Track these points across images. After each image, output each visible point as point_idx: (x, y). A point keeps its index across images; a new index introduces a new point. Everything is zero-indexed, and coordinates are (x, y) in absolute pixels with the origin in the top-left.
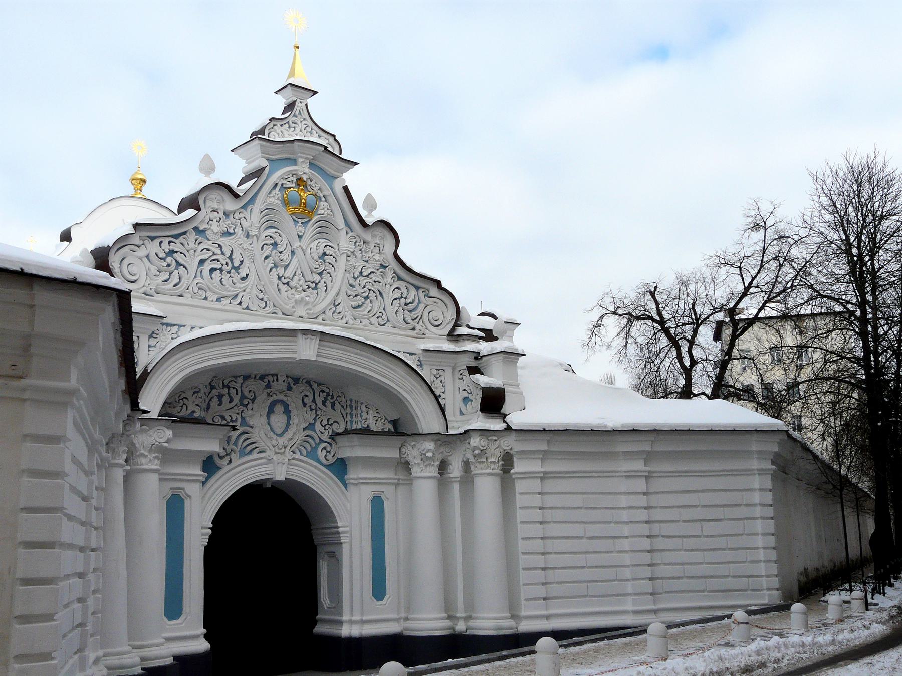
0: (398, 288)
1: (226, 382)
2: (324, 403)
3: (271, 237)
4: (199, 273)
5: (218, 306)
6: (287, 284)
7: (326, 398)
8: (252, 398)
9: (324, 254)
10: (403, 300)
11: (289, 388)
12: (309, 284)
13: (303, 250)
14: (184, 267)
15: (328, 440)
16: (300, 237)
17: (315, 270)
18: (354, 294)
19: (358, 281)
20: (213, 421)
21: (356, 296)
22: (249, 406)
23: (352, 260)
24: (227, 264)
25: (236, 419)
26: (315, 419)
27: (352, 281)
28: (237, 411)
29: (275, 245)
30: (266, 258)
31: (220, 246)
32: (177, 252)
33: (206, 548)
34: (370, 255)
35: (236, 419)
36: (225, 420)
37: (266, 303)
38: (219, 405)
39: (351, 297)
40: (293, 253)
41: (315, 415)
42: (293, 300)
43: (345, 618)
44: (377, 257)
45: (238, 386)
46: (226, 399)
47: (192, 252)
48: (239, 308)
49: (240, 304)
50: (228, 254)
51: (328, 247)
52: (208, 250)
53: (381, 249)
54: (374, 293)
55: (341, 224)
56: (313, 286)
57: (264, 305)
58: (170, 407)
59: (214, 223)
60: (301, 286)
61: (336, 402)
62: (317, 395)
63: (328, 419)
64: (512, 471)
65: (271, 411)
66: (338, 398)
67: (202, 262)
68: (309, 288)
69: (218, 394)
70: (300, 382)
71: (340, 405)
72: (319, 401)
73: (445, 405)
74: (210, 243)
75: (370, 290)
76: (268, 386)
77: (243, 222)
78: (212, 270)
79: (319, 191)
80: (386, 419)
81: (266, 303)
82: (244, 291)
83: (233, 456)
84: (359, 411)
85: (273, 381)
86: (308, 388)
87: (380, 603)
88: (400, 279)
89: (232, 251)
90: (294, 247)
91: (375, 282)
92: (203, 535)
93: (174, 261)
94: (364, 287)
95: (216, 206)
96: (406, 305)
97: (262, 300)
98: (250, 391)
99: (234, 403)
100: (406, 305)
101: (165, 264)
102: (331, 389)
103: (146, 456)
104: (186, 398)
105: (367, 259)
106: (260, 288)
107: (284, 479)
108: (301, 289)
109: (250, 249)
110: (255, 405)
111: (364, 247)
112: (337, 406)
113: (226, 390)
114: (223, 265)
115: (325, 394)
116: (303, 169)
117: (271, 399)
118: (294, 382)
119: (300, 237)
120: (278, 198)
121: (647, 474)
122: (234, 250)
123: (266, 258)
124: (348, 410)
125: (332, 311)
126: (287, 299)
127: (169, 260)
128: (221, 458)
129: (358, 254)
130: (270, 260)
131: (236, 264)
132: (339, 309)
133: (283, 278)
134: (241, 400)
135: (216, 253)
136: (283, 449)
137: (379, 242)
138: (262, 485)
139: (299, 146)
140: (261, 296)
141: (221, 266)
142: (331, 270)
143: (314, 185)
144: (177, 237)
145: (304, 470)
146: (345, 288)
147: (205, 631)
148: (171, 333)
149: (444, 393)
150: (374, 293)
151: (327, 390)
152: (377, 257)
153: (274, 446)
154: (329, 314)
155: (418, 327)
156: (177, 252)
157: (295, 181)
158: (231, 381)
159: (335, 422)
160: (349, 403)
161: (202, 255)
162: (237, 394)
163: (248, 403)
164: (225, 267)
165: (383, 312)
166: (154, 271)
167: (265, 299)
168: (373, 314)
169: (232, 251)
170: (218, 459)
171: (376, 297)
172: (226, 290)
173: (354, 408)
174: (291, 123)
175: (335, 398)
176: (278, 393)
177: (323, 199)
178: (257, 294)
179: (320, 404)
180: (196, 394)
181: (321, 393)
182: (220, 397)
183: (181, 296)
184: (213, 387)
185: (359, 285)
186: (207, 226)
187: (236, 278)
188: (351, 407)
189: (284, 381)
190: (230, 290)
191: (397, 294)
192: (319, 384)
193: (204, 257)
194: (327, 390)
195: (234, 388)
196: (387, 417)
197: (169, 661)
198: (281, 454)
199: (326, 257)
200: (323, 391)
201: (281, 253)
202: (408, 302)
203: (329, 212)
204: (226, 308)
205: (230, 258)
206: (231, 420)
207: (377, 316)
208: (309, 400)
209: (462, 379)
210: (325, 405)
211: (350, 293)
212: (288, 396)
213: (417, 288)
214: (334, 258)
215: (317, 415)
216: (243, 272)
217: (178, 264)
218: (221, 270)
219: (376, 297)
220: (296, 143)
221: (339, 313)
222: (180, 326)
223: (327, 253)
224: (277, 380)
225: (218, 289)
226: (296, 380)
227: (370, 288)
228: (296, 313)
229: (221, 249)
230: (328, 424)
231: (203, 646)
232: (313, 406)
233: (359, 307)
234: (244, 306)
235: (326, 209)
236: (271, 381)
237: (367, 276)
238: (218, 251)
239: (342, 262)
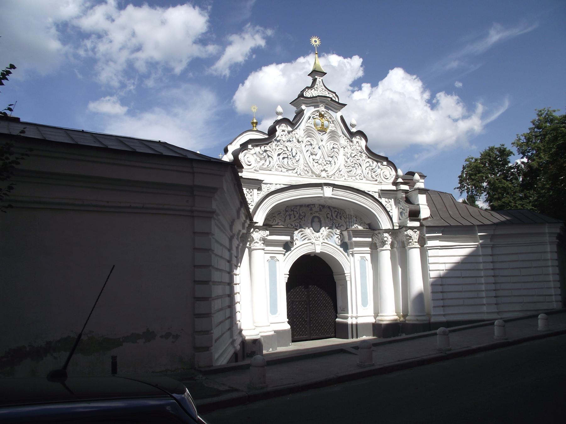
0: (368, 162)
1: (292, 209)
2: (336, 217)
3: (309, 141)
4: (278, 160)
5: (287, 174)
6: (317, 162)
9: (333, 148)
10: (371, 168)
11: (320, 210)
12: (327, 162)
13: (324, 147)
14: (271, 157)
15: (339, 234)
16: (322, 141)
17: (329, 155)
18: (348, 166)
19: (349, 159)
20: (288, 226)
21: (349, 166)
22: (303, 219)
25: (297, 225)
26: (332, 224)
27: (346, 159)
28: (298, 222)
29: (311, 145)
30: (307, 151)
31: (287, 147)
32: (268, 151)
33: (287, 283)
34: (354, 147)
35: (297, 225)
36: (292, 226)
37: (308, 172)
38: (290, 219)
39: (346, 167)
40: (319, 148)
41: (332, 222)
42: (320, 170)
43: (350, 314)
44: (358, 148)
45: (297, 210)
46: (292, 216)
47: (274, 150)
48: (296, 175)
49: (297, 173)
50: (290, 150)
52: (281, 149)
53: (360, 144)
54: (357, 164)
55: (341, 134)
56: (329, 163)
57: (307, 173)
58: (268, 221)
59: (283, 137)
60: (323, 163)
61: (342, 216)
62: (333, 213)
63: (339, 224)
64: (425, 246)
65: (312, 221)
66: (343, 214)
67: (279, 155)
68: (327, 164)
69: (289, 214)
70: (325, 207)
72: (334, 215)
73: (392, 215)
74: (282, 146)
75: (355, 163)
76: (311, 209)
77: (296, 135)
78: (284, 158)
80: (365, 223)
81: (308, 172)
82: (298, 167)
83: (296, 242)
84: (352, 219)
85: (313, 207)
86: (329, 210)
87: (365, 308)
88: (369, 158)
89: (292, 149)
90: (320, 145)
91: (357, 159)
92: (285, 277)
93: (267, 155)
94: (352, 162)
95: (284, 128)
96: (372, 169)
97: (306, 170)
98: (303, 212)
99: (296, 218)
100: (372, 169)
101: (263, 157)
103: (258, 243)
104: (275, 217)
105: (353, 149)
106: (305, 165)
107: (320, 252)
108: (323, 165)
109: (300, 147)
111: (351, 144)
112: (343, 218)
113: (292, 212)
114: (288, 156)
115: (337, 212)
116: (322, 109)
119: (322, 141)
121: (492, 246)
122: (293, 148)
123: (307, 151)
124: (348, 220)
125: (338, 174)
126: (317, 169)
127: (265, 154)
129: (349, 147)
130: (309, 152)
132: (341, 173)
133: (315, 160)
134: (299, 217)
135: (285, 150)
136: (319, 239)
137: (358, 141)
138: (310, 255)
139: (319, 99)
140: (305, 169)
141: (287, 156)
142: (337, 155)
143: (327, 116)
144: (267, 144)
145: (329, 248)
146: (344, 163)
147: (288, 320)
148: (267, 187)
149: (392, 210)
150: (357, 164)
151: (338, 211)
152: (358, 148)
153: (315, 237)
154: (336, 175)
155: (378, 180)
156: (268, 151)
157: (318, 115)
159: (341, 225)
160: (347, 216)
161: (279, 151)
162: (297, 213)
163: (302, 218)
164: (289, 156)
166: (258, 159)
167: (308, 170)
168: (357, 175)
169: (292, 149)
170: (290, 243)
171: (358, 166)
172: (290, 167)
173: (350, 219)
174: (315, 88)
175: (341, 214)
176: (315, 213)
177: (332, 122)
178: (304, 168)
179: (334, 217)
180: (279, 215)
182: (290, 215)
183: (270, 170)
184: (286, 211)
185: (350, 161)
186: (281, 138)
187: (294, 161)
188: (349, 218)
189: (318, 207)
190: (292, 167)
191: (368, 164)
192: (334, 208)
193: (280, 152)
194: (338, 211)
196: (366, 222)
197: (273, 333)
198: (318, 240)
200: (335, 211)
201: (314, 148)
202: (373, 168)
203: (335, 128)
204: (290, 175)
206: (295, 226)
207: (359, 175)
209: (399, 203)
210: (337, 218)
211: (346, 165)
212: (320, 214)
213: (377, 162)
214: (338, 149)
216: (297, 158)
217: (269, 156)
218: (287, 157)
219: (358, 166)
220: (318, 98)
222: (270, 184)
223: (335, 147)
224: (315, 207)
225: (286, 166)
226: (323, 206)
227: (355, 162)
228: (321, 176)
229: (287, 148)
230: (338, 226)
231: (288, 327)
232: (331, 219)
233: (350, 171)
234: (298, 173)
235: (333, 127)
236: (312, 206)
237: (354, 157)
238: (285, 149)
239: (342, 151)
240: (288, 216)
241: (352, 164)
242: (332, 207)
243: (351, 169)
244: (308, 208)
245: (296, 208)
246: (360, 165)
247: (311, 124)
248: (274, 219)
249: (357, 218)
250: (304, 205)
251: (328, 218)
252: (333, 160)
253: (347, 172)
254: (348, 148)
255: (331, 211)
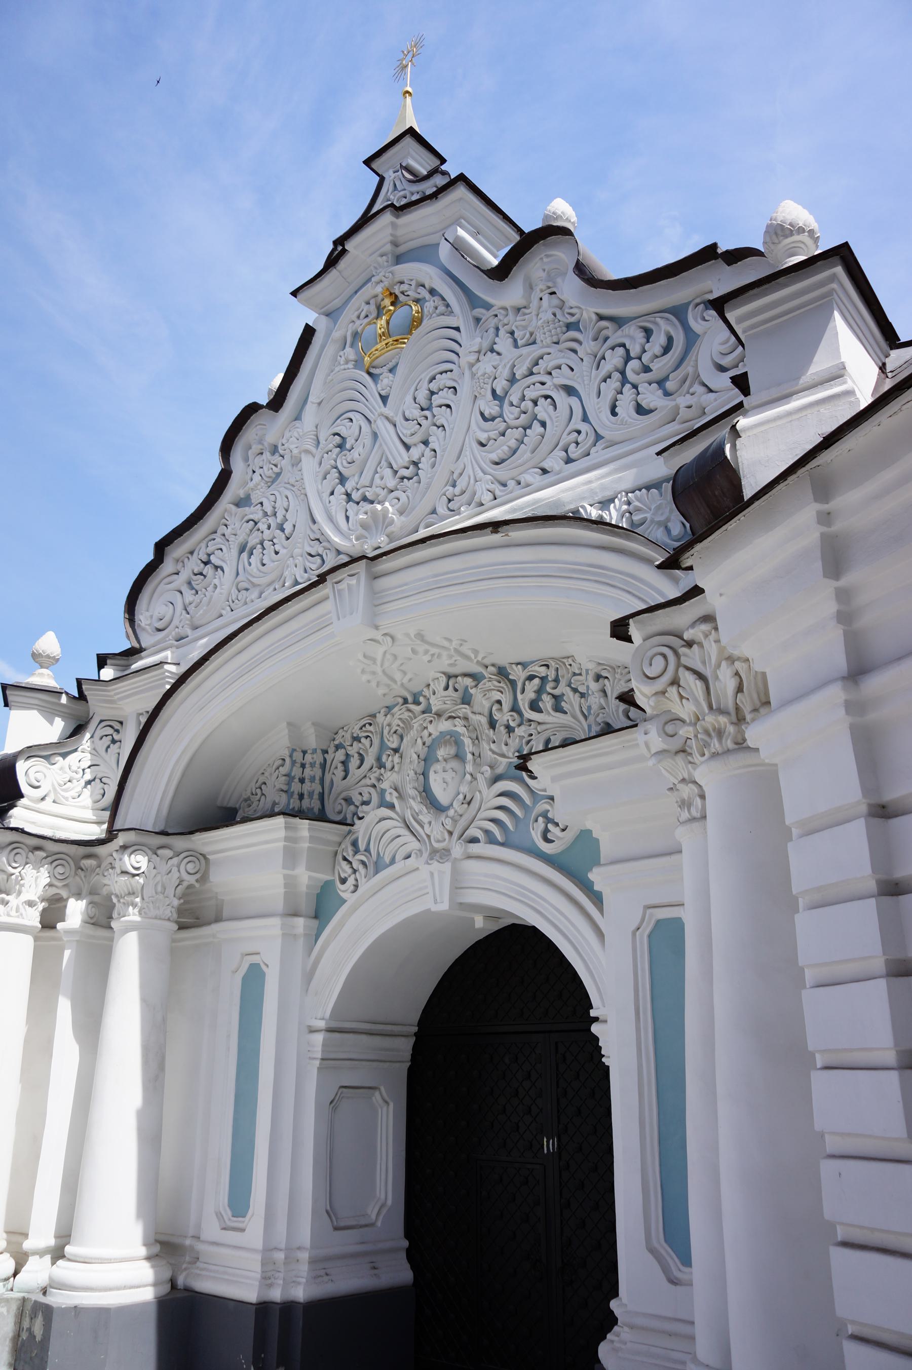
7: (539, 691)
8: (394, 746)
13: (387, 418)
23: (487, 364)
24: (269, 527)
27: (491, 408)
36: (353, 803)
46: (354, 762)
50: (269, 511)
51: (438, 376)
54: (547, 397)
69: (343, 758)
71: (577, 694)
72: (523, 701)
79: (421, 289)
94: (523, 398)
102: (553, 664)
104: (265, 783)
110: (396, 759)
112: (571, 701)
115: (536, 681)
117: (426, 733)
118: (473, 684)
119: (384, 399)
120: (347, 362)
125: (445, 499)
128: (343, 881)
129: (504, 344)
131: (279, 520)
134: (379, 759)
158: (364, 726)
165: (584, 427)
175: (563, 683)
177: (428, 296)
181: (527, 683)
182: (345, 763)
184: (338, 747)
189: (446, 688)
192: (524, 665)
195: (367, 737)
199: (434, 397)
200: (531, 678)
205: (275, 514)
208: (500, 710)
210: (540, 711)
211: (483, 437)
215: (522, 737)
221: (463, 492)
224: (434, 693)
232: (512, 724)
240: (340, 765)
241: (516, 411)
242: (518, 664)
243: (513, 443)
244: (412, 707)
245: (370, 724)
246: (570, 391)
247: (347, 362)
248: (263, 794)
249: (607, 678)
250: (400, 700)
251: (492, 724)
252: (428, 453)
253: (489, 468)
254: (499, 354)
255: (513, 683)
